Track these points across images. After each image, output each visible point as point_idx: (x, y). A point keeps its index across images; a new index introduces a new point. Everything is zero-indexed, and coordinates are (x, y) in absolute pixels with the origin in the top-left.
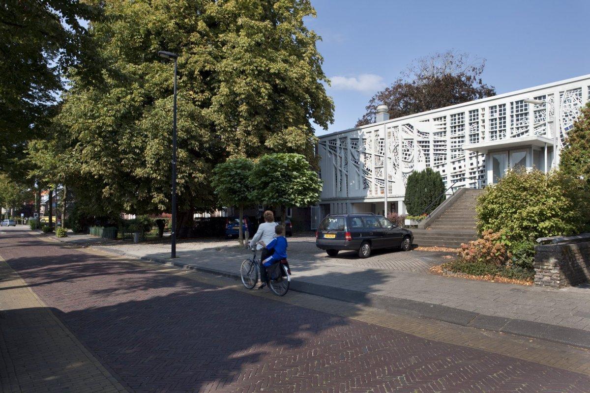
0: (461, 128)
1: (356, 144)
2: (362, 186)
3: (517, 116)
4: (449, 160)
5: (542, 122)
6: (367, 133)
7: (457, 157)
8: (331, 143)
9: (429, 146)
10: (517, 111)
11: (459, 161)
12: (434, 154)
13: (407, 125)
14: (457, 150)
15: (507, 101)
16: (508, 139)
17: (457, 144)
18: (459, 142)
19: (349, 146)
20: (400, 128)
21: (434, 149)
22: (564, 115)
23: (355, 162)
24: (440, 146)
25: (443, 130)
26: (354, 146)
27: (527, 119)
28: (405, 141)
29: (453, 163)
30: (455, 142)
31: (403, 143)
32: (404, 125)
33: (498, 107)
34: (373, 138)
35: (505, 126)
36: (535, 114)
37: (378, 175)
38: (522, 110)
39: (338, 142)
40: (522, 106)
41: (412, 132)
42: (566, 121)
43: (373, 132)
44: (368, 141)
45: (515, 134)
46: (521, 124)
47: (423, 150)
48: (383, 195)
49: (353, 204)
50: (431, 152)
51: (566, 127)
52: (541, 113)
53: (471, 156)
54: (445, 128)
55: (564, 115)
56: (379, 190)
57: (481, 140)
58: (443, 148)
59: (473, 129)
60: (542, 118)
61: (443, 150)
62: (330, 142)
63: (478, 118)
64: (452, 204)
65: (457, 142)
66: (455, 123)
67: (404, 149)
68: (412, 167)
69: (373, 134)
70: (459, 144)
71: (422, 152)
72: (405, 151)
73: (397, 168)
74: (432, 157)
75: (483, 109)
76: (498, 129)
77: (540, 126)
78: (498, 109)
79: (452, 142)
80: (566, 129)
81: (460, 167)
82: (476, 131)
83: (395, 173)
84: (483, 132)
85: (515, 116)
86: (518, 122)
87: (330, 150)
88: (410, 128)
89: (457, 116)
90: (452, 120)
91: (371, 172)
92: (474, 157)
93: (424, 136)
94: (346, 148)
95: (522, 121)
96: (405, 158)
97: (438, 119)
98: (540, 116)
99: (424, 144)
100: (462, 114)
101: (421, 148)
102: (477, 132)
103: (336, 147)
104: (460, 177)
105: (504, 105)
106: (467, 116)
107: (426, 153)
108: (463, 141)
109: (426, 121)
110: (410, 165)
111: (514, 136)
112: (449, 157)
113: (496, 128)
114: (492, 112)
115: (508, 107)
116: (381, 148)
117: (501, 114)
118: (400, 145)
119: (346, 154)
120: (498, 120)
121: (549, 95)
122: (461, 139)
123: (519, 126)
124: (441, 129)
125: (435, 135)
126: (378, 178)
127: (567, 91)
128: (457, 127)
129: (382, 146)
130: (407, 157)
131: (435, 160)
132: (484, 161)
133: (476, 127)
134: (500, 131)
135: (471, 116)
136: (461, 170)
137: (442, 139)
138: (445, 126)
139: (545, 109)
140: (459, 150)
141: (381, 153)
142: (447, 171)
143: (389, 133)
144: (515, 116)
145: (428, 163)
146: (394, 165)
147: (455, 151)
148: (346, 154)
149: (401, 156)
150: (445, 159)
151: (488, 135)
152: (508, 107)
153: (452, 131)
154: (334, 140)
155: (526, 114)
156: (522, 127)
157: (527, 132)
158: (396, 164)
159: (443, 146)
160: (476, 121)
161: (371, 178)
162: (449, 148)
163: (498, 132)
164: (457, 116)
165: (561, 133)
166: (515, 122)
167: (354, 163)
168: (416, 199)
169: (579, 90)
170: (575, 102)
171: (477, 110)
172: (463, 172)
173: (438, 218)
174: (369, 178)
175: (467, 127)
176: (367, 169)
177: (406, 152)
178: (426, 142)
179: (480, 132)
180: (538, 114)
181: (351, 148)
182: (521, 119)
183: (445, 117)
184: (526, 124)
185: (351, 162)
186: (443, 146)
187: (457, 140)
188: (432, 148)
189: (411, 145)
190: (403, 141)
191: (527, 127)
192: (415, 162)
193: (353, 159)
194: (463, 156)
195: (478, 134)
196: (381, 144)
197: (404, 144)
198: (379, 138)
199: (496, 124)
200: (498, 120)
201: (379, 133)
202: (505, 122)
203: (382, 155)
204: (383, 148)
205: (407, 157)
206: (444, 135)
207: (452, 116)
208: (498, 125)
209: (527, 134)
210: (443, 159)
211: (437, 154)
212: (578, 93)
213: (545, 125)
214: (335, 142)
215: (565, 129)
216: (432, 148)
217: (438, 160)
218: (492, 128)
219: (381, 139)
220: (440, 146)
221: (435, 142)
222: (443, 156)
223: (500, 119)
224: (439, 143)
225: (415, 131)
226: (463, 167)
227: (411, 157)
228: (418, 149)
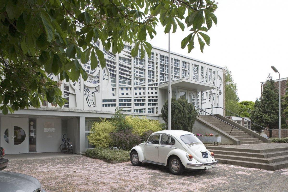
11: (140, 89)
24: (125, 70)
30: (137, 72)
52: (184, 72)
68: (95, 83)
70: (140, 75)
82: (151, 68)
93: (109, 56)
108: (142, 73)
122: (141, 71)
124: (126, 56)
127: (195, 65)
128: (138, 60)
131: (120, 82)
133: (152, 66)
137: (127, 65)
140: (140, 80)
147: (137, 79)
172: (143, 98)
178: (111, 62)
182: (176, 71)
184: (178, 75)
187: (138, 70)
217: (123, 82)
221: (120, 65)
224: (124, 68)
226: (142, 94)
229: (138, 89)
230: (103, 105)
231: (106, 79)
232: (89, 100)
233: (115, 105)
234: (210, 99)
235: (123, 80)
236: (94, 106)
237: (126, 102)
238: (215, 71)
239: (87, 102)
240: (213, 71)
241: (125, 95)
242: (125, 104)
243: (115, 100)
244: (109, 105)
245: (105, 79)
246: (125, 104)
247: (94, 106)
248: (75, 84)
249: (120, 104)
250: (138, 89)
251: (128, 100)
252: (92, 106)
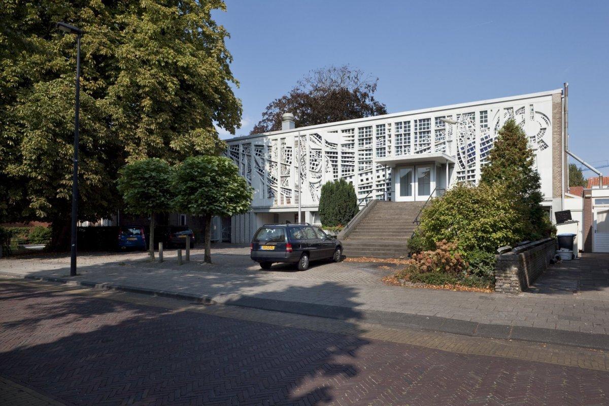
0: (368, 141)
1: (260, 151)
2: (267, 195)
3: (420, 133)
4: (356, 172)
5: (442, 141)
6: (272, 140)
7: (365, 170)
8: (233, 149)
9: (337, 157)
10: (420, 129)
11: (366, 173)
12: (342, 165)
13: (315, 134)
14: (365, 163)
15: (411, 119)
16: (411, 155)
17: (365, 157)
18: (366, 155)
19: (253, 153)
20: (308, 137)
21: (342, 161)
22: (461, 135)
23: (260, 170)
24: (348, 157)
25: (351, 142)
26: (258, 153)
27: (429, 137)
28: (313, 151)
29: (361, 175)
30: (363, 155)
31: (311, 153)
32: (312, 135)
33: (403, 123)
34: (279, 146)
35: (409, 142)
36: (436, 132)
37: (284, 185)
38: (424, 128)
39: (241, 148)
40: (424, 125)
41: (320, 142)
42: (462, 141)
43: (279, 140)
44: (273, 149)
45: (418, 150)
46: (424, 141)
47: (331, 160)
48: (289, 205)
49: (256, 213)
50: (339, 163)
51: (462, 146)
52: (441, 133)
53: (378, 169)
54: (353, 140)
55: (461, 135)
56: (285, 199)
57: (387, 154)
58: (350, 159)
59: (379, 143)
60: (442, 137)
61: (351, 162)
62: (232, 147)
63: (384, 133)
64: (366, 215)
65: (365, 155)
66: (363, 136)
67: (311, 158)
68: (319, 177)
69: (279, 142)
71: (330, 163)
72: (313, 161)
73: (304, 178)
74: (340, 168)
75: (390, 125)
76: (403, 144)
77: (441, 144)
78: (403, 125)
79: (360, 155)
80: (463, 148)
81: (367, 179)
82: (383, 145)
84: (389, 147)
85: (418, 133)
86: (421, 139)
87: (231, 156)
88: (318, 138)
89: (365, 130)
90: (360, 133)
91: (277, 180)
92: (380, 170)
94: (249, 154)
95: (424, 139)
96: (313, 168)
97: (346, 131)
98: (440, 135)
99: (332, 155)
100: (370, 127)
101: (329, 158)
102: (383, 146)
103: (238, 154)
104: (366, 188)
105: (409, 122)
106: (374, 129)
107: (334, 164)
108: (370, 154)
109: (334, 132)
110: (318, 175)
111: (418, 152)
112: (356, 168)
113: (401, 143)
114: (398, 128)
115: (412, 124)
116: (287, 156)
117: (405, 131)
118: (308, 154)
119: (249, 161)
120: (403, 135)
121: (448, 117)
122: (368, 152)
123: (422, 142)
125: (342, 147)
126: (283, 187)
127: (463, 114)
128: (365, 140)
129: (288, 155)
130: (315, 167)
131: (343, 171)
132: (390, 174)
134: (405, 147)
135: (378, 130)
136: (368, 182)
137: (351, 150)
138: (353, 139)
139: (445, 129)
140: (367, 163)
141: (287, 162)
142: (356, 181)
143: (297, 141)
144: (418, 133)
145: (336, 174)
146: (301, 174)
147: (363, 163)
148: (249, 161)
149: (308, 165)
150: (353, 171)
151: (393, 149)
152: (412, 124)
153: (360, 144)
154: (236, 146)
155: (428, 132)
156: (424, 144)
157: (429, 149)
159: (351, 157)
160: (383, 135)
161: (277, 187)
162: (356, 160)
163: (403, 147)
164: (365, 129)
165: (458, 151)
166: (418, 139)
167: (258, 171)
168: (331, 210)
169: (473, 114)
170: (470, 125)
171: (384, 125)
172: (370, 184)
173: (355, 229)
174: (275, 187)
175: (374, 140)
176: (272, 178)
177: (314, 162)
178: (334, 153)
179: (386, 146)
180: (438, 133)
181: (255, 155)
183: (353, 130)
184: (428, 141)
185: (255, 170)
186: (351, 157)
187: (365, 152)
188: (340, 159)
189: (319, 155)
190: (311, 150)
191: (429, 144)
192: (323, 173)
193: (257, 166)
194: (370, 168)
195: (384, 148)
196: (287, 153)
197: (312, 154)
198: (285, 146)
199: (401, 139)
200: (403, 135)
201: (285, 141)
202: (409, 139)
203: (288, 164)
204: (290, 156)
205: (315, 167)
206: (352, 148)
207: (360, 129)
208: (403, 141)
209: (429, 151)
210: (351, 171)
211: (344, 165)
212: (472, 116)
213: (444, 143)
214: (237, 148)
215: (461, 148)
216: (340, 159)
217: (346, 171)
218: (398, 143)
219: (287, 147)
220: (348, 157)
221: (343, 153)
222: (351, 167)
223: (405, 135)
224: (347, 155)
225: (323, 141)
226: (370, 179)
227: (319, 167)
228: (326, 159)
229: (364, 175)
238: (524, 107)
240: (515, 110)
250: (364, 175)
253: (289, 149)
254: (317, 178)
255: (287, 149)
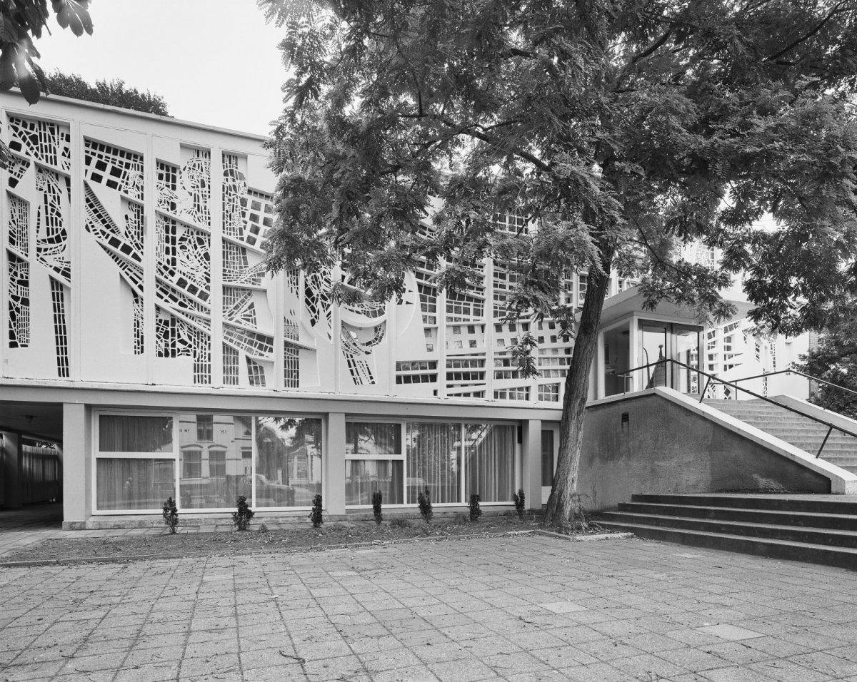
1: (115, 172)
37: (238, 316)
43: (216, 157)
68: (375, 315)
69: (216, 166)
73: (319, 306)
83: (313, 322)
91: (204, 296)
116: (250, 223)
131: (449, 309)
150: (477, 313)
158: (315, 292)
167: (106, 242)
176: (182, 283)
193: (99, 226)
201: (241, 167)
217: (458, 310)
222: (472, 303)
230: (399, 380)
231: (407, 303)
232: (355, 366)
233: (434, 378)
234: (758, 350)
235: (460, 303)
236: (371, 381)
237: (470, 369)
239: (352, 371)
241: (466, 349)
242: (466, 376)
243: (433, 365)
244: (416, 379)
245: (404, 302)
246: (466, 376)
247: (371, 381)
248: (316, 320)
249: (449, 376)
251: (473, 363)
252: (366, 381)
253: (257, 199)
254: (367, 314)
255: (250, 199)
